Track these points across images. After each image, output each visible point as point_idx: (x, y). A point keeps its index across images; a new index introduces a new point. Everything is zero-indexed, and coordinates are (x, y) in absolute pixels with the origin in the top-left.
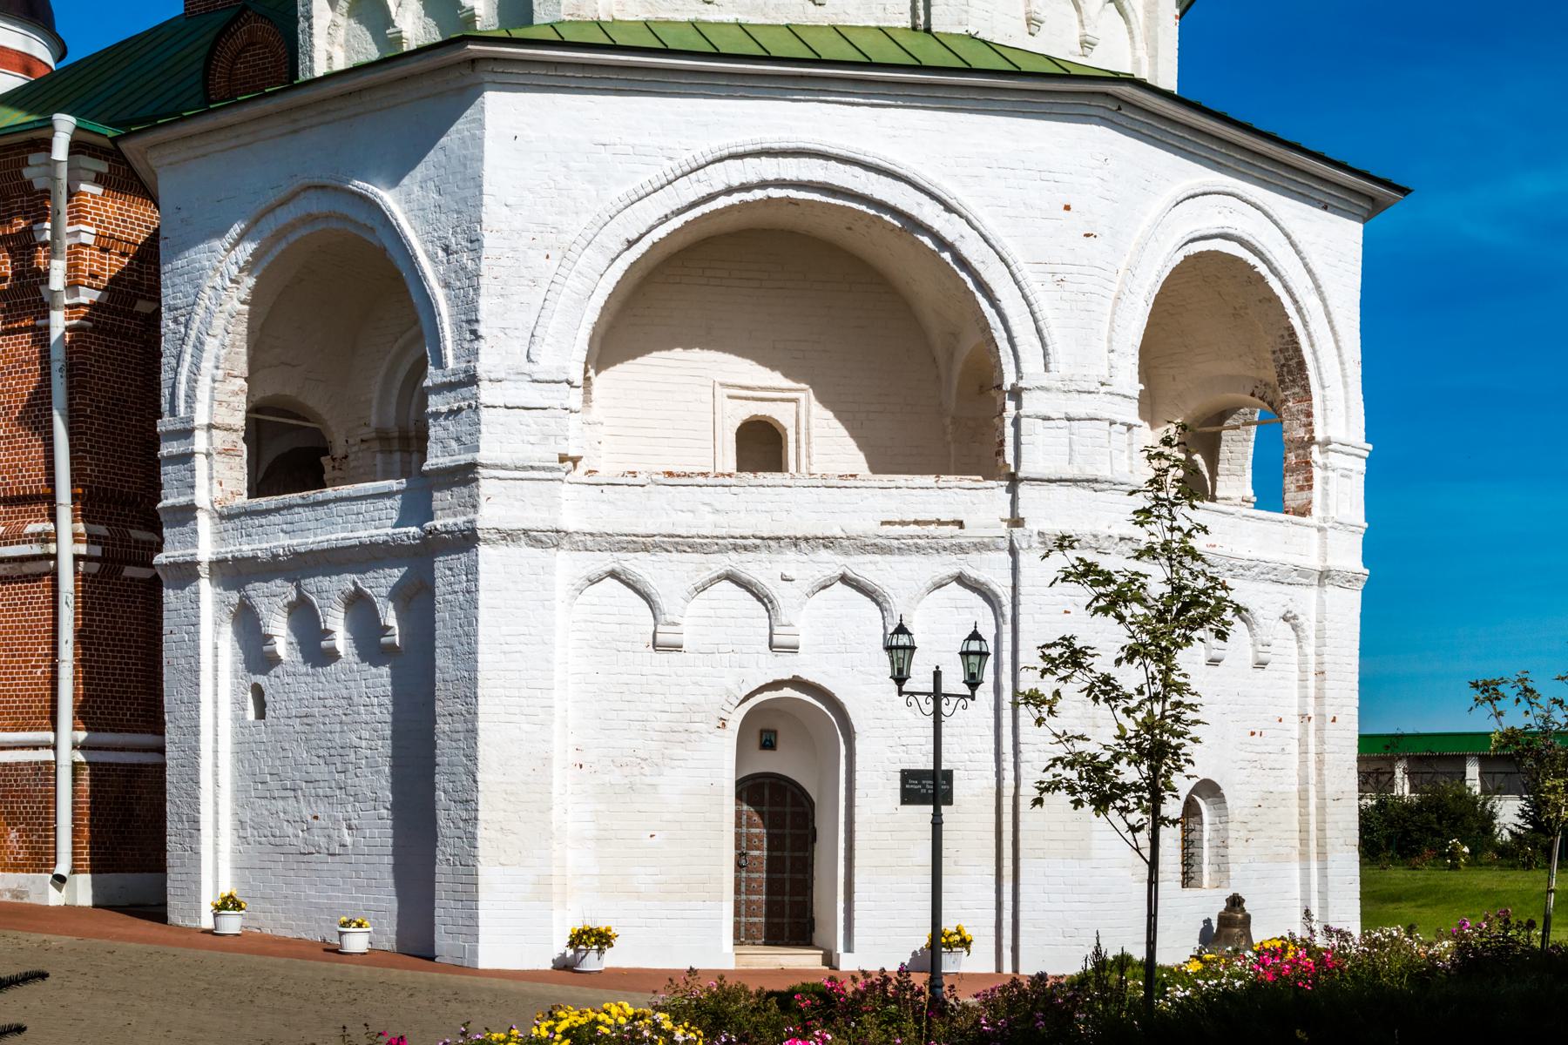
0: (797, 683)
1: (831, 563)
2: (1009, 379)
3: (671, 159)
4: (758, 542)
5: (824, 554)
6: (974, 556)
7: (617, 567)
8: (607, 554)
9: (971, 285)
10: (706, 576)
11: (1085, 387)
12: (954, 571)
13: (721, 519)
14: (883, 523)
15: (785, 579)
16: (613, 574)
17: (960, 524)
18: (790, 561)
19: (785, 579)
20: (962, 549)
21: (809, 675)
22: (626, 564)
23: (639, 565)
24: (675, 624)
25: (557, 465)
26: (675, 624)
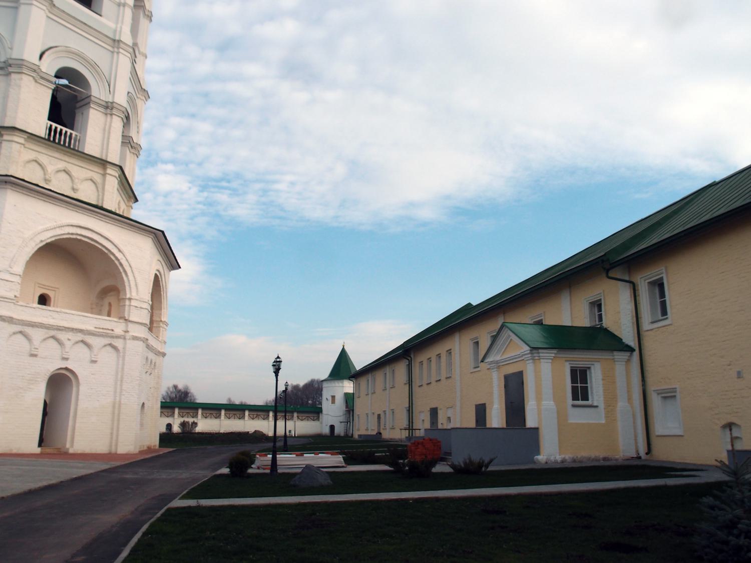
0: (66, 369)
1: (80, 337)
2: (128, 296)
3: (56, 222)
4: (63, 328)
5: (79, 334)
6: (115, 340)
7: (23, 330)
8: (20, 326)
9: (122, 270)
10: (47, 336)
11: (145, 301)
12: (109, 343)
13: (53, 321)
14: (95, 328)
15: (69, 340)
16: (21, 332)
17: (113, 330)
18: (70, 335)
19: (69, 340)
20: (112, 337)
21: (70, 367)
22: (25, 330)
23: (29, 330)
24: (37, 349)
25: (14, 298)
26: (37, 349)
